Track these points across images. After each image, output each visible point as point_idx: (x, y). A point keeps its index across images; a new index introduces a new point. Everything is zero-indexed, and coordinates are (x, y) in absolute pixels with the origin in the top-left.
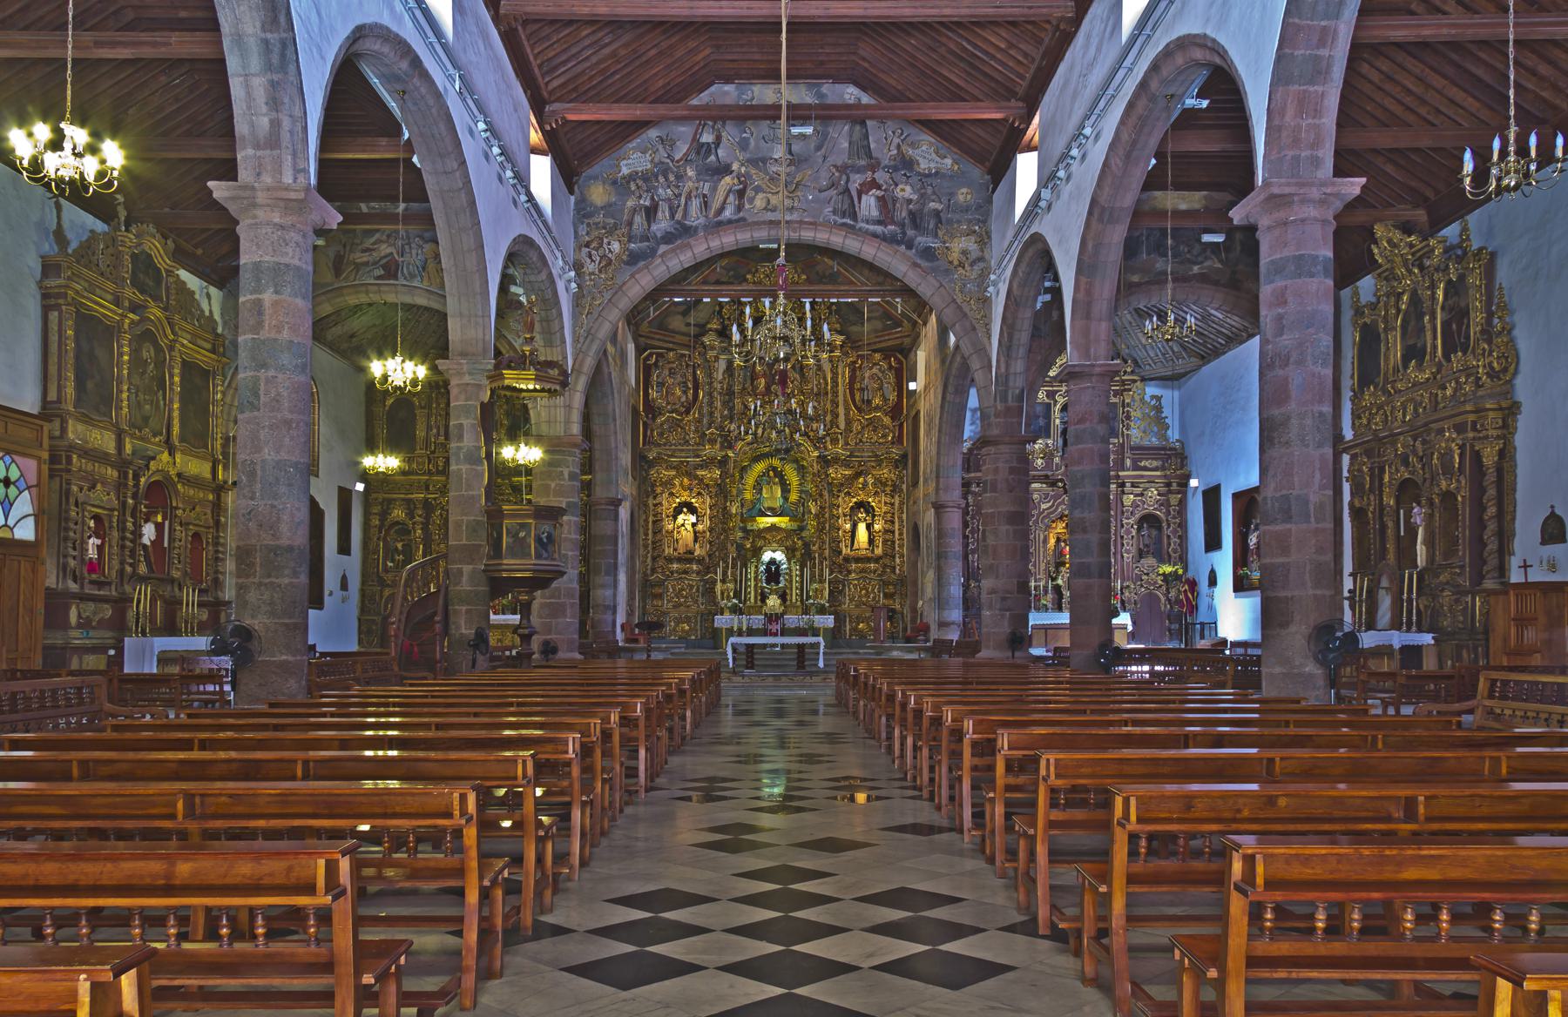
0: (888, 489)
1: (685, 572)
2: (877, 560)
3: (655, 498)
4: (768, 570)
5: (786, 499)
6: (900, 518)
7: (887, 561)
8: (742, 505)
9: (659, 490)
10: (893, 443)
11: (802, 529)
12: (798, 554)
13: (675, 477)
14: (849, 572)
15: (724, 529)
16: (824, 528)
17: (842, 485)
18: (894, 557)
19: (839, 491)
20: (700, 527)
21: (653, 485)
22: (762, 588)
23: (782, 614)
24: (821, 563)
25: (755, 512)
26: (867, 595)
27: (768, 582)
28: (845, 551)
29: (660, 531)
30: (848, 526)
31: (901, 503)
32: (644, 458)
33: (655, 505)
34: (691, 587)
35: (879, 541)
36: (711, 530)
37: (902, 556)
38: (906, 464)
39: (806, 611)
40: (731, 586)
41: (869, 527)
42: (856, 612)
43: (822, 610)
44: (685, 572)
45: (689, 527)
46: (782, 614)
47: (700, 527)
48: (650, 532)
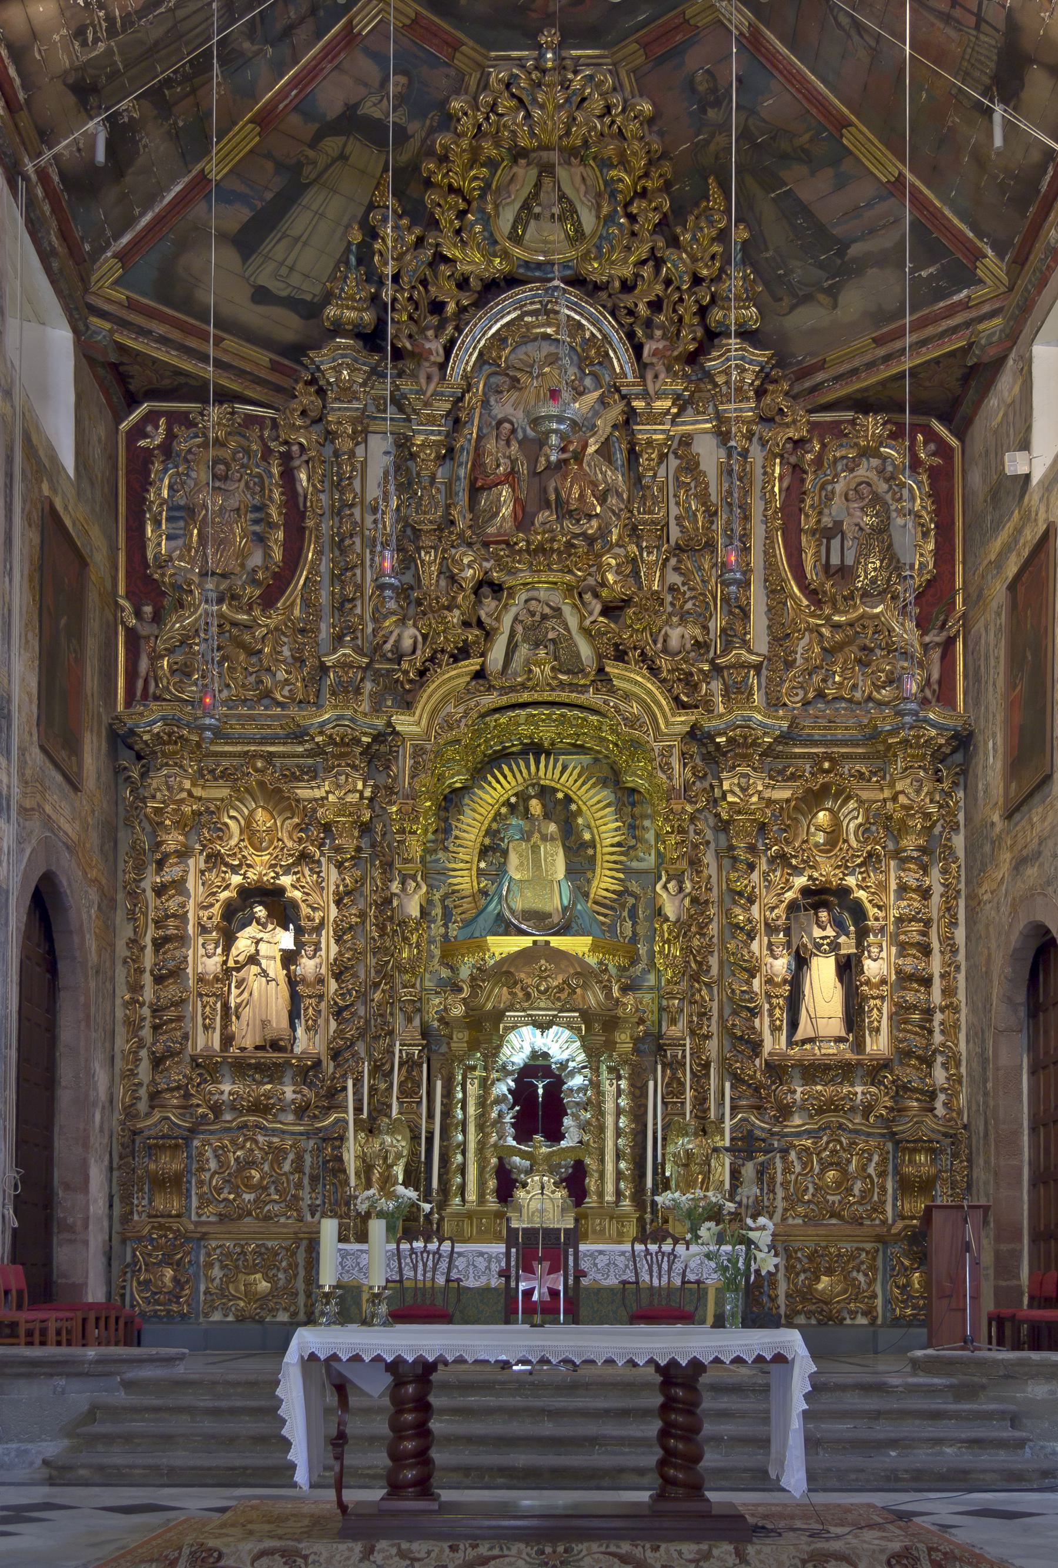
0: (910, 843)
2: (876, 1071)
3: (160, 864)
6: (948, 942)
7: (909, 1074)
9: (173, 840)
13: (226, 804)
14: (785, 1111)
16: (703, 967)
17: (763, 827)
20: (307, 966)
26: (843, 1184)
27: (523, 1133)
28: (773, 1044)
29: (177, 973)
30: (781, 965)
31: (950, 895)
33: (160, 891)
36: (340, 971)
44: (260, 1108)
45: (275, 969)
48: (147, 979)
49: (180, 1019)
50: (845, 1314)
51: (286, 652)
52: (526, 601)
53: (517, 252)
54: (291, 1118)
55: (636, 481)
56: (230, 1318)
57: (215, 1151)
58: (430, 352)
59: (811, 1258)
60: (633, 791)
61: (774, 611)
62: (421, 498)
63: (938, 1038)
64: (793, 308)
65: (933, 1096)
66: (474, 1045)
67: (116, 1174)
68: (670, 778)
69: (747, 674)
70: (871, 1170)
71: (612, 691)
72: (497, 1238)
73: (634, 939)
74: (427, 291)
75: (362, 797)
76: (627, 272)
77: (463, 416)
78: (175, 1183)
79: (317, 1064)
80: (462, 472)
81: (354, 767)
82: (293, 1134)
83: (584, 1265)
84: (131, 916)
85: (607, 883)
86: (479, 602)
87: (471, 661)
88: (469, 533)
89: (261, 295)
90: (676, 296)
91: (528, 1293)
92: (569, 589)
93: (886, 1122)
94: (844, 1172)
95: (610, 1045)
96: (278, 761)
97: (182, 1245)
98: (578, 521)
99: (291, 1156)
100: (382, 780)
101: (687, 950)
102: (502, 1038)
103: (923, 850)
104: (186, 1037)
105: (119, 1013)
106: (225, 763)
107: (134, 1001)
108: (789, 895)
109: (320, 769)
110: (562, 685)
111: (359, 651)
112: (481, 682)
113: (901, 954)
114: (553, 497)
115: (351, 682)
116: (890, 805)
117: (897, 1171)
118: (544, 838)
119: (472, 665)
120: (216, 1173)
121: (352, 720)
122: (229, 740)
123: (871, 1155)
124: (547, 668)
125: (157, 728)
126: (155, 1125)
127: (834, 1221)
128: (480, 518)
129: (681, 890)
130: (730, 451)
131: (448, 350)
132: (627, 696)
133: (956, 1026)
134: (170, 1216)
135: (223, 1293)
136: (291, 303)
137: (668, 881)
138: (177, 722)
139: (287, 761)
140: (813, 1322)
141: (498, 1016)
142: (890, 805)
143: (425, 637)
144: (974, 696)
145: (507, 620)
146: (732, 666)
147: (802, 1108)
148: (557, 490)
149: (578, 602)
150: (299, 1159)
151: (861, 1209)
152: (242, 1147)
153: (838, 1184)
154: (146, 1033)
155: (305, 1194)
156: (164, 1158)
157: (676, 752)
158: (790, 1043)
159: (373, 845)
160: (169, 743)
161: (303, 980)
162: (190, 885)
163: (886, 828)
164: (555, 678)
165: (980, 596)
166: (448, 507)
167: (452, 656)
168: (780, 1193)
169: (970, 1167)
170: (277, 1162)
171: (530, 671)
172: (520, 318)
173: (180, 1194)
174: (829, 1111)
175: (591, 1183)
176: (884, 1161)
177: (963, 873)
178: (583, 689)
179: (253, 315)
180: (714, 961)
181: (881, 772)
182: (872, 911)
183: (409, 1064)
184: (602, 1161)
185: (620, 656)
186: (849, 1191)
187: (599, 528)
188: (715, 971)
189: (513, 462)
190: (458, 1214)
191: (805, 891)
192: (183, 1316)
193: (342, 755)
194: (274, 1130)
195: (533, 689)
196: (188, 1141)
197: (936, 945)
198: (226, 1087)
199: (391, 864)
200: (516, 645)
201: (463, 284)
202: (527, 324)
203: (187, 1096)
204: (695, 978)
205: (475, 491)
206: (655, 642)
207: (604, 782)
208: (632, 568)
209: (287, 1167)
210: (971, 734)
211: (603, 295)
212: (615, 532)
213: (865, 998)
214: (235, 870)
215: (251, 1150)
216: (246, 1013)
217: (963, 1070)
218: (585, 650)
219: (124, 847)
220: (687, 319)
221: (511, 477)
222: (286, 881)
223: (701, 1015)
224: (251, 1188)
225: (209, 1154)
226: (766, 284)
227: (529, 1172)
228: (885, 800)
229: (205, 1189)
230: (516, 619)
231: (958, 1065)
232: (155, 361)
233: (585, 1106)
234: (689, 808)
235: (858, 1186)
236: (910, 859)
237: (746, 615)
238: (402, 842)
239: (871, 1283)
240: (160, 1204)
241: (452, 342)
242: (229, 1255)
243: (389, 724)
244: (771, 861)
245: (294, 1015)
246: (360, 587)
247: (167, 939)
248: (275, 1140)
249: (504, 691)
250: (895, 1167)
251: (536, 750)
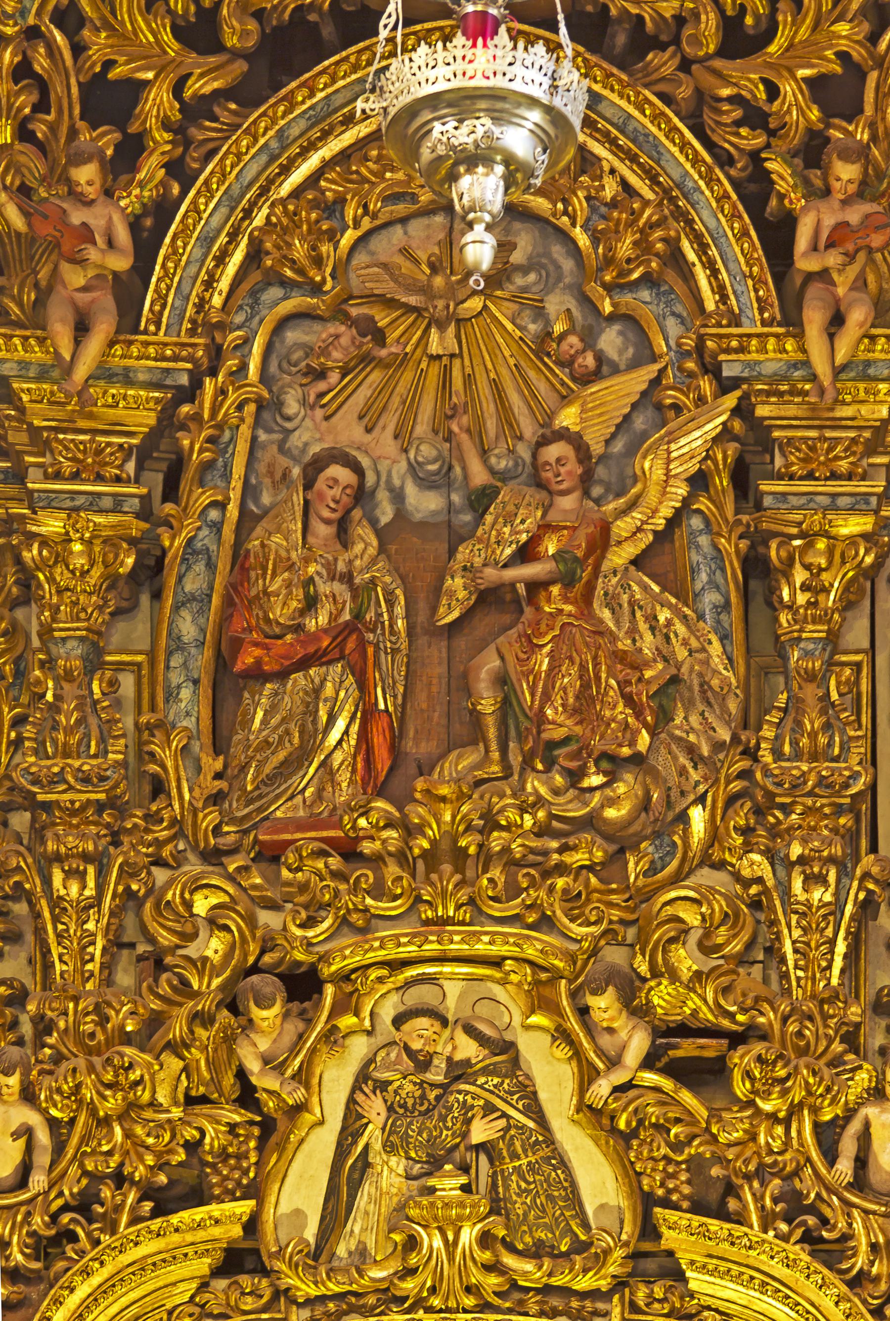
52: (398, 1021)
58: (86, 234)
62: (54, 708)
80: (187, 628)
87: (214, 1209)
88: (209, 819)
98: (575, 777)
112: (245, 1281)
114: (487, 705)
148: (502, 680)
149: (574, 1024)
187: (645, 805)
200: (364, 1164)
206: (831, 1157)
212: (698, 817)
230: (362, 1077)
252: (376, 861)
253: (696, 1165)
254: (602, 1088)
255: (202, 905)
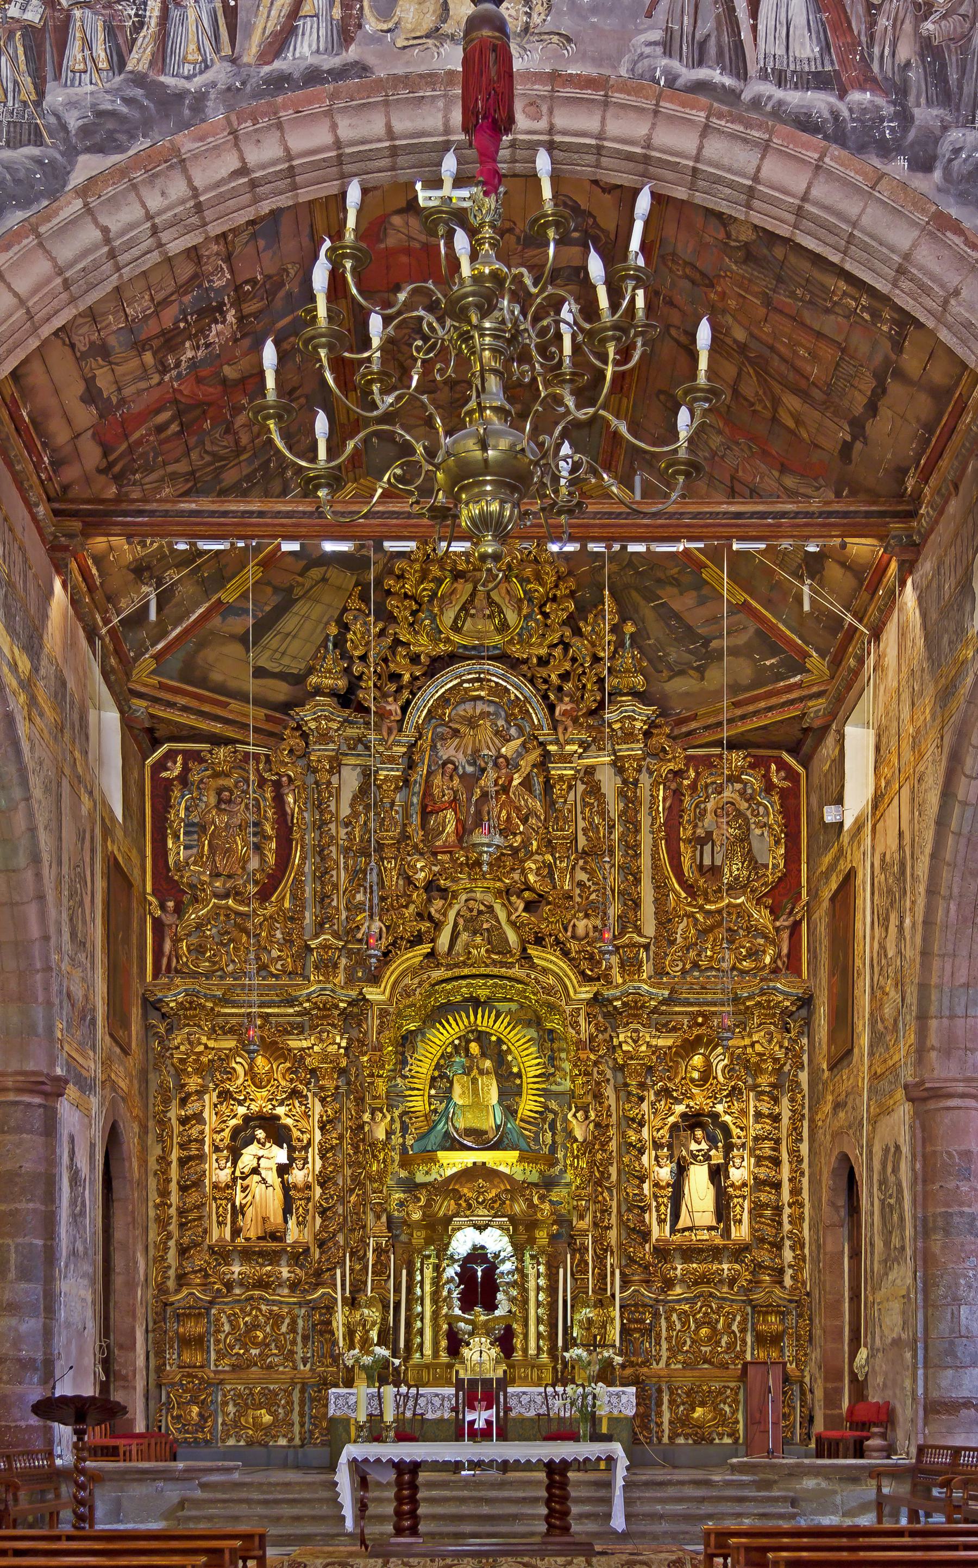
1: (262, 1284)
2: (738, 1253)
3: (183, 1102)
4: (466, 1276)
5: (510, 1112)
7: (764, 1256)
8: (404, 1129)
9: (193, 1083)
10: (775, 971)
11: (548, 1183)
12: (542, 1236)
13: (234, 1052)
14: (669, 1284)
15: (357, 1182)
16: (605, 1175)
17: (650, 1070)
18: (778, 1246)
19: (642, 1086)
20: (297, 1176)
21: (179, 1073)
22: (452, 1320)
23: (503, 1383)
24: (600, 1260)
25: (435, 1138)
26: (714, 1339)
27: (467, 1303)
28: (657, 1232)
29: (198, 1183)
30: (665, 1173)
31: (796, 1117)
32: (152, 1005)
33: (184, 1121)
34: (277, 1320)
35: (742, 1209)
36: (324, 1180)
37: (798, 1244)
38: (808, 1022)
39: (564, 1375)
40: (372, 1314)
41: (716, 1174)
42: (685, 1381)
43: (606, 1374)
44: (262, 1284)
45: (272, 1177)
46: (503, 1383)
47: (297, 1176)
48: (173, 1187)
49: (200, 1218)
50: (715, 1436)
51: (279, 935)
52: (466, 901)
53: (456, 638)
54: (286, 1291)
55: (550, 804)
56: (242, 1443)
57: (228, 1317)
58: (390, 712)
59: (688, 1394)
60: (551, 1031)
61: (660, 902)
62: (383, 819)
63: (787, 1227)
64: (670, 678)
65: (781, 1271)
66: (429, 1241)
67: (151, 1335)
68: (578, 1033)
69: (638, 951)
70: (735, 1328)
71: (533, 966)
72: (448, 1383)
73: (553, 1148)
74: (388, 666)
75: (340, 1047)
76: (543, 651)
77: (415, 757)
78: (199, 1342)
79: (307, 1251)
80: (415, 800)
81: (334, 1026)
82: (288, 1303)
83: (512, 1402)
84: (160, 1139)
85: (532, 1106)
86: (429, 901)
88: (421, 845)
89: (260, 673)
90: (580, 671)
91: (472, 1423)
92: (499, 893)
93: (747, 1291)
94: (714, 1329)
95: (532, 1241)
96: (273, 1020)
97: (205, 1389)
99: (287, 1321)
100: (355, 1034)
101: (592, 1163)
102: (450, 1237)
103: (774, 1086)
104: (205, 1231)
105: (152, 1213)
106: (233, 1021)
107: (163, 1204)
108: (672, 1119)
109: (307, 1027)
110: (494, 963)
111: (336, 935)
113: (758, 1165)
115: (330, 960)
116: (749, 1050)
117: (753, 1329)
118: (481, 1072)
119: (425, 948)
120: (229, 1334)
121: (332, 991)
122: (235, 1004)
123: (735, 1316)
124: (483, 950)
125: (180, 998)
126: (183, 1299)
127: (706, 1366)
128: (430, 834)
129: (587, 1118)
130: (625, 782)
131: (404, 709)
132: (545, 971)
133: (801, 1218)
134: (195, 1367)
135: (236, 1423)
136: (281, 676)
137: (577, 1112)
138: (197, 994)
139: (280, 1019)
140: (690, 1441)
141: (448, 1220)
142: (749, 1050)
143: (388, 928)
144: (813, 971)
145: (452, 914)
146: (627, 946)
147: (682, 1281)
150: (294, 1322)
151: (727, 1357)
152: (250, 1314)
153: (710, 1339)
154: (173, 1227)
155: (299, 1349)
156: (190, 1324)
157: (582, 1012)
158: (673, 1231)
159: (348, 1083)
160: (190, 1009)
161: (295, 1187)
162: (206, 1115)
163: (746, 1068)
164: (489, 958)
165: (817, 893)
166: (405, 825)
167: (409, 941)
168: (665, 1345)
169: (811, 1324)
170: (276, 1325)
171: (470, 953)
172: (460, 684)
173: (202, 1350)
174: (703, 1283)
175: (518, 1342)
176: (744, 1320)
177: (806, 1101)
178: (510, 966)
179: (251, 686)
180: (613, 1170)
181: (742, 1025)
182: (735, 1131)
183: (378, 1250)
184: (526, 1325)
185: (539, 941)
186: (718, 1343)
187: (523, 841)
188: (614, 1177)
189: (456, 792)
190: (418, 1365)
191: (684, 1116)
192: (207, 1442)
193: (324, 1017)
194: (274, 1301)
195: (472, 965)
196: (208, 1310)
197: (785, 1156)
198: (236, 1269)
199: (363, 1099)
201: (415, 659)
202: (466, 689)
203: (207, 1276)
204: (599, 1183)
205: (425, 815)
206: (566, 930)
207: (528, 1024)
208: (548, 871)
209: (284, 1329)
210: (811, 996)
211: (525, 667)
212: (535, 843)
213: (731, 1197)
214: (241, 1103)
215: (257, 1316)
216: (250, 1212)
217: (807, 1251)
218: (512, 937)
219: (153, 1086)
220: (589, 686)
221: (454, 803)
222: (280, 1111)
223: (602, 1212)
224: (257, 1345)
225: (224, 1319)
226: (650, 661)
227: (472, 1334)
228: (745, 1047)
229: (221, 1346)
230: (458, 914)
231: (802, 1247)
232: (176, 722)
233: (514, 1284)
234: (592, 1057)
235: (725, 1339)
236: (762, 1093)
237: (637, 905)
238: (372, 1083)
239: (734, 1412)
240: (186, 1358)
241: (408, 702)
242: (240, 1396)
243: (361, 993)
244: (657, 1094)
245: (287, 1210)
246: (336, 886)
247: (190, 1158)
248: (275, 1308)
249: (449, 967)
250: (753, 1324)
251: (476, 1003)
252: (462, 863)
253: (536, 933)
254: (513, 917)
255: (419, 865)
